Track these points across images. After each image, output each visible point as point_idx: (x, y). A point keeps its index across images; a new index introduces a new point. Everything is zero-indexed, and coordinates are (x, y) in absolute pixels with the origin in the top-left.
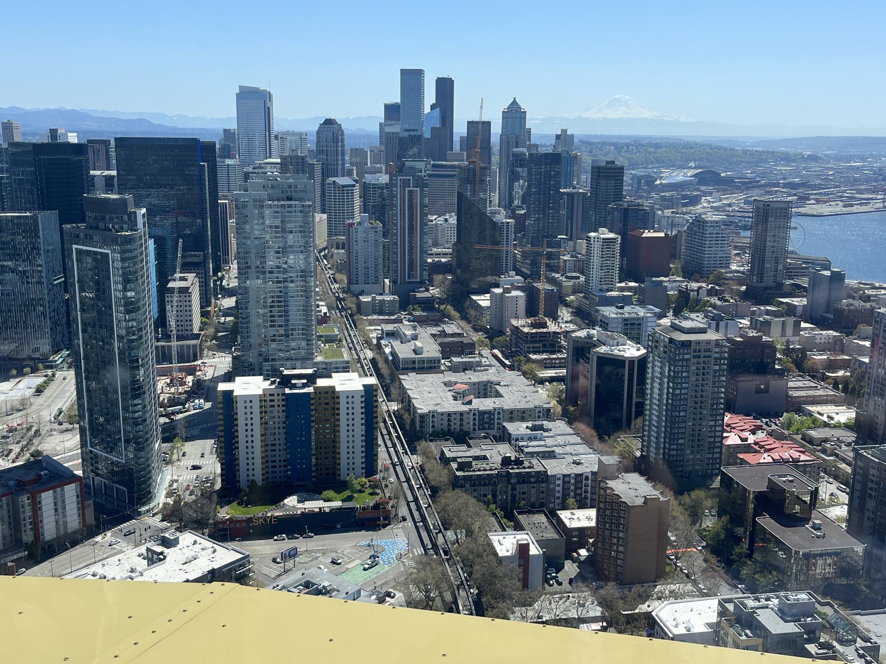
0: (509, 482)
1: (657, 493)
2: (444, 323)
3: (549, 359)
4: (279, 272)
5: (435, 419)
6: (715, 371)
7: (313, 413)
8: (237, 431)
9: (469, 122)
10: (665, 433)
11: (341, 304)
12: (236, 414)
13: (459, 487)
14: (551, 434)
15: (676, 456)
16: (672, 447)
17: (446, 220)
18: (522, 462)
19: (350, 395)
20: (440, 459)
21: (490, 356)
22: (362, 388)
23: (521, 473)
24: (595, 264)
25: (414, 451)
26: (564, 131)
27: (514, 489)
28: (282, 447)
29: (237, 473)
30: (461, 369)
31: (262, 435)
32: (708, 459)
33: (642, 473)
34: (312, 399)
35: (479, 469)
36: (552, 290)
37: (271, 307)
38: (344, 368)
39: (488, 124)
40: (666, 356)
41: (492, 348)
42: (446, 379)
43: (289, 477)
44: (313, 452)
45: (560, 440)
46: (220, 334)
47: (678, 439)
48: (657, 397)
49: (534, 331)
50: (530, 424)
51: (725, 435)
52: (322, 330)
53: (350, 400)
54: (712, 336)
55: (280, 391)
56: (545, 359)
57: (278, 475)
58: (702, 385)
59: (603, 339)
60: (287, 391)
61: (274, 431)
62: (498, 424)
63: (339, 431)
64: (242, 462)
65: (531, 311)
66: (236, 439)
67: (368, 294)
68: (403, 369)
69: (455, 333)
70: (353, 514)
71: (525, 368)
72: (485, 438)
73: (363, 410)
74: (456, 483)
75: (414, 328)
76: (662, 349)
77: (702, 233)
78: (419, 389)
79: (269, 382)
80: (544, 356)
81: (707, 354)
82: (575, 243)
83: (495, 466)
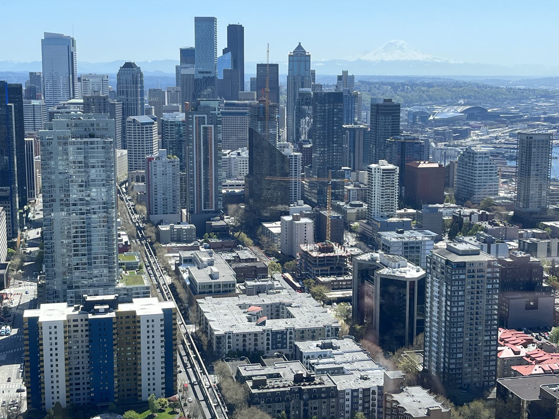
0: (301, 398)
1: (439, 404)
2: (239, 249)
3: (337, 281)
4: (82, 204)
5: (231, 340)
6: (488, 290)
7: (115, 337)
8: (42, 356)
9: (258, 65)
10: (445, 349)
11: (141, 233)
12: (42, 339)
13: (254, 404)
14: (340, 351)
15: (455, 369)
16: (452, 361)
17: (239, 154)
18: (313, 379)
19: (151, 319)
20: (236, 377)
21: (282, 280)
22: (163, 313)
24: (376, 192)
25: (211, 371)
26: (345, 73)
27: (306, 405)
28: (85, 370)
29: (42, 396)
31: (66, 359)
32: (485, 371)
33: (424, 387)
34: (114, 323)
35: (273, 386)
36: (338, 217)
37: (74, 237)
39: (276, 66)
40: (444, 276)
41: (284, 271)
42: (241, 302)
43: (92, 399)
44: (116, 374)
45: (349, 357)
46: (26, 264)
47: (457, 353)
48: (436, 315)
49: (322, 255)
50: (320, 342)
51: (499, 348)
52: (123, 258)
53: (150, 323)
54: (484, 257)
55: (83, 317)
56: (333, 281)
57: (82, 397)
58: (477, 303)
59: (385, 262)
60: (90, 316)
61: (78, 355)
62: (290, 343)
63: (140, 354)
64: (47, 385)
65: (319, 236)
66: (41, 364)
67: (167, 223)
68: (200, 293)
69: (249, 259)
71: (314, 289)
72: (278, 356)
73: (163, 333)
74: (251, 401)
75: (210, 254)
76: (439, 270)
77: (473, 164)
78: (215, 312)
79: (73, 308)
80: (332, 278)
81: (480, 274)
82: (358, 174)
83: (288, 383)
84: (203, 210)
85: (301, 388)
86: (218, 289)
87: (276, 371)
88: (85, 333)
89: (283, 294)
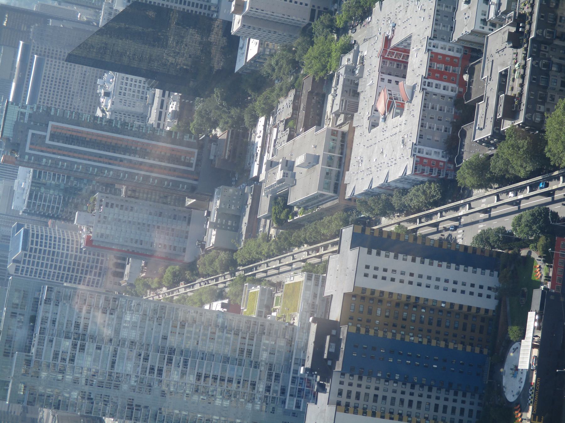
17: (107, 94)
22: (356, 250)
23: (539, 21)
30: (353, 100)
38: (317, 285)
42: (366, 123)
60: (339, 367)
67: (205, 232)
70: (552, 297)
78: (373, 169)
84: (193, 169)
85: (532, 39)
86: (336, 161)
87: (496, 78)
88: (364, 382)
89: (365, 53)
